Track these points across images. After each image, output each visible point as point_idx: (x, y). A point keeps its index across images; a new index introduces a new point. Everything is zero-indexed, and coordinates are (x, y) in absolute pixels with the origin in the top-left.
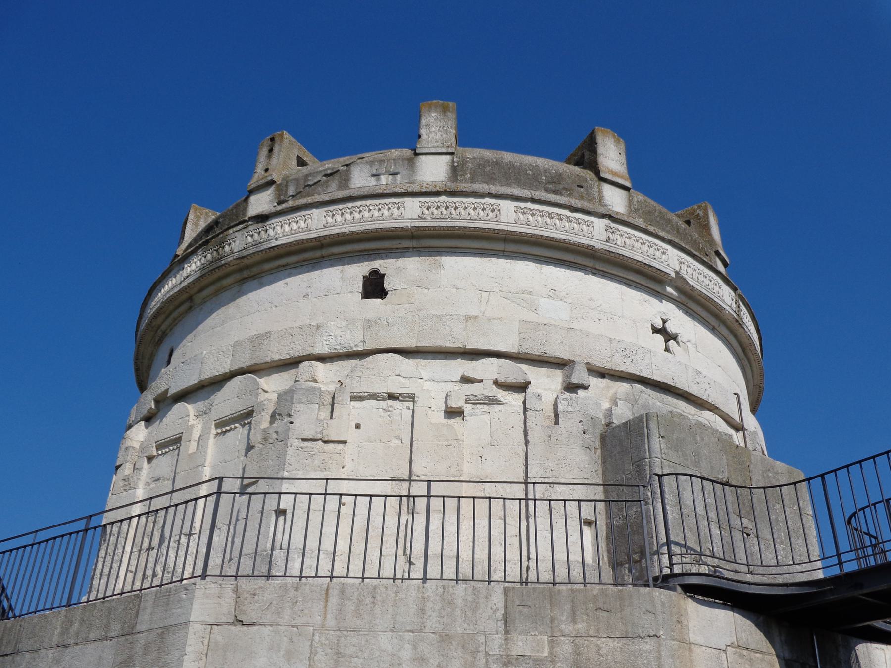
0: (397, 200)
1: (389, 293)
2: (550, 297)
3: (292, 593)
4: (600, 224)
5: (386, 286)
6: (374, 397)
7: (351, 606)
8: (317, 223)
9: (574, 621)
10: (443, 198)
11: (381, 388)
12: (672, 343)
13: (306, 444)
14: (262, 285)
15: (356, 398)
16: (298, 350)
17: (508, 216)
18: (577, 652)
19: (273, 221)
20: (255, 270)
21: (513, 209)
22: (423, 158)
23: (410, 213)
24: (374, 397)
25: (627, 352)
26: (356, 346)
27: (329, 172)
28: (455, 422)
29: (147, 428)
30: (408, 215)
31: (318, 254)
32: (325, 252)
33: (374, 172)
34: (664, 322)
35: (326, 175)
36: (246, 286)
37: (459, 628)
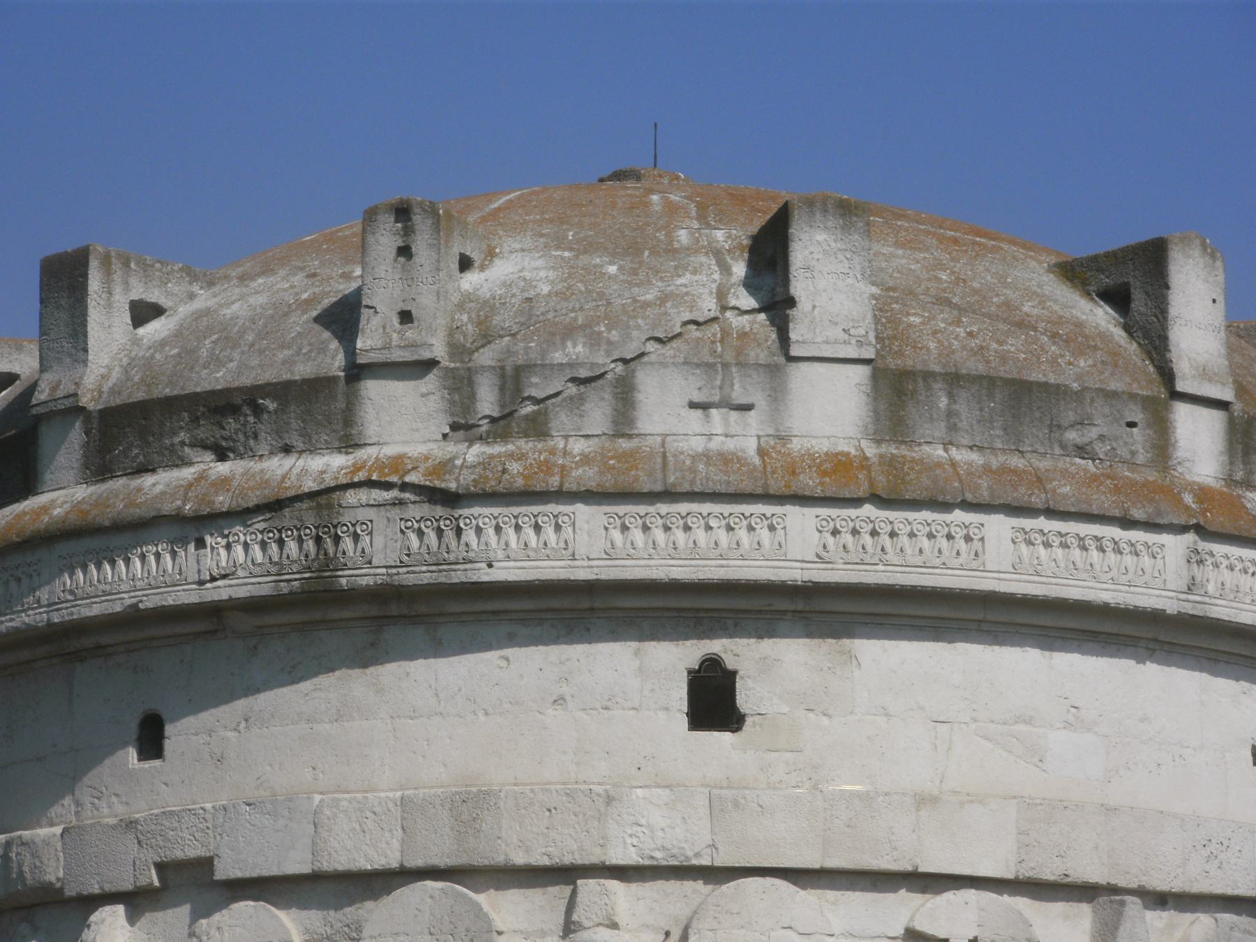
0: (768, 509)
1: (749, 721)
2: (1068, 725)
4: (1175, 546)
5: (744, 700)
8: (589, 543)
10: (868, 510)
14: (438, 649)
16: (568, 851)
17: (1001, 553)
19: (476, 510)
20: (422, 609)
21: (1009, 534)
22: (804, 366)
23: (795, 544)
25: (1213, 847)
26: (697, 855)
27: (583, 373)
29: (132, 918)
30: (795, 551)
32: (598, 603)
33: (697, 397)
35: (574, 380)
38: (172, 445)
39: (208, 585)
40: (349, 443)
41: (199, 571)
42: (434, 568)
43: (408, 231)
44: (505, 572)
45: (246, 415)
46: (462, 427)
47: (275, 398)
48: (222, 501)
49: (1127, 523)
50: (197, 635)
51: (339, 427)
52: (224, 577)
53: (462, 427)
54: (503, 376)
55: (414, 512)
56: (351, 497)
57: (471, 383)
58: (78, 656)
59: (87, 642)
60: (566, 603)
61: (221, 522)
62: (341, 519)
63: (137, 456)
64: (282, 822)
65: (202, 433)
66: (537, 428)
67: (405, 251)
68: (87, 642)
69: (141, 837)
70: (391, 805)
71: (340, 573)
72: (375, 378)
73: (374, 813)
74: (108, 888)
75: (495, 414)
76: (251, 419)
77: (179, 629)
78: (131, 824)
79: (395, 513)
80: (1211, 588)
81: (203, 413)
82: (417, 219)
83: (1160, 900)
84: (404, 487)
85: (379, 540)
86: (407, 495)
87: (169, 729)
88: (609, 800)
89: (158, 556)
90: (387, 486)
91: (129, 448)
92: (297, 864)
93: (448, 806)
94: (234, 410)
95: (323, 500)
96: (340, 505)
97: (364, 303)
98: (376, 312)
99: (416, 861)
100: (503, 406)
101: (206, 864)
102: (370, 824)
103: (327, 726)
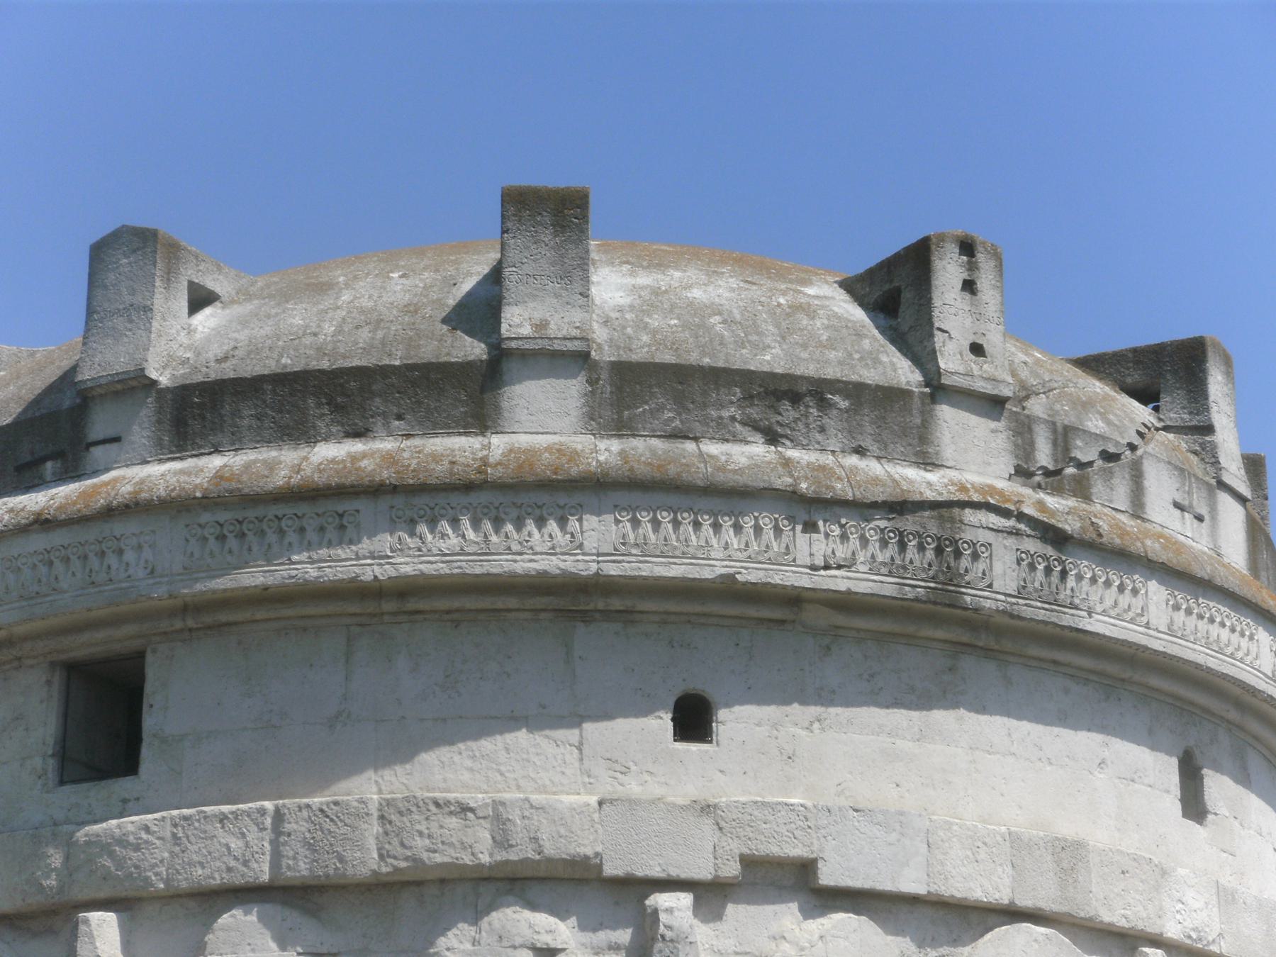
1: (1210, 817)
36: (968, 663)
38: (721, 418)
39: (822, 572)
40: (928, 462)
41: (811, 555)
42: (1047, 606)
43: (972, 267)
44: (1098, 625)
45: (807, 406)
46: (1022, 473)
47: (847, 396)
48: (841, 488)
50: (761, 621)
51: (915, 442)
52: (839, 567)
53: (1022, 473)
54: (1055, 431)
55: (1033, 546)
56: (969, 515)
57: (1030, 430)
58: (585, 617)
59: (616, 604)
61: (837, 510)
62: (963, 535)
63: (671, 420)
64: (894, 836)
65: (754, 412)
66: (1081, 490)
67: (969, 286)
68: (616, 604)
69: (723, 824)
70: (999, 838)
71: (964, 590)
72: (952, 405)
73: (985, 844)
74: (674, 872)
75: (1051, 467)
76: (814, 411)
77: (752, 612)
78: (707, 809)
79: (1011, 542)
81: (759, 393)
82: (981, 257)
84: (1021, 517)
85: (998, 568)
86: (1022, 526)
87: (722, 714)
89: (758, 530)
90: (1005, 513)
91: (661, 408)
92: (912, 882)
93: (1050, 850)
94: (796, 399)
95: (944, 511)
96: (961, 522)
97: (936, 325)
98: (951, 338)
100: (1056, 461)
102: (982, 855)
103: (910, 744)
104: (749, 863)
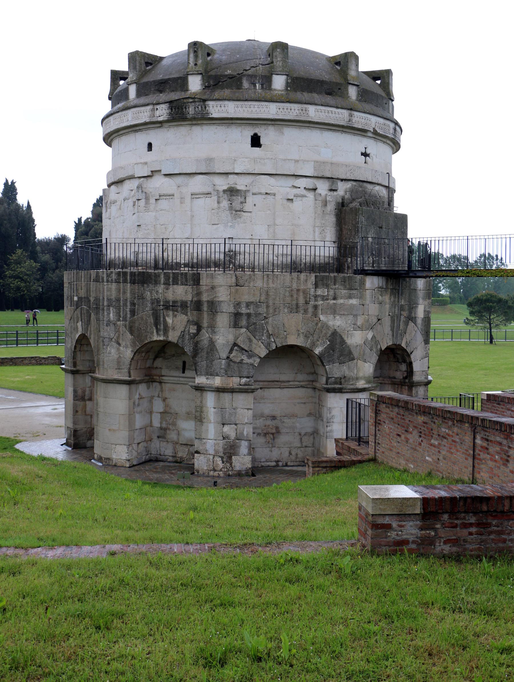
2: (325, 147)
3: (253, 277)
5: (262, 142)
6: (260, 194)
7: (271, 281)
9: (335, 285)
11: (264, 191)
12: (367, 158)
13: (239, 213)
15: (253, 194)
18: (335, 294)
21: (314, 110)
24: (260, 194)
28: (289, 204)
31: (231, 122)
32: (233, 122)
34: (366, 148)
37: (302, 287)
49: (337, 108)
60: (227, 122)
80: (353, 121)
83: (342, 180)
88: (235, 160)
99: (199, 172)
101: (160, 171)
104: (152, 171)
